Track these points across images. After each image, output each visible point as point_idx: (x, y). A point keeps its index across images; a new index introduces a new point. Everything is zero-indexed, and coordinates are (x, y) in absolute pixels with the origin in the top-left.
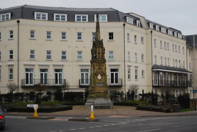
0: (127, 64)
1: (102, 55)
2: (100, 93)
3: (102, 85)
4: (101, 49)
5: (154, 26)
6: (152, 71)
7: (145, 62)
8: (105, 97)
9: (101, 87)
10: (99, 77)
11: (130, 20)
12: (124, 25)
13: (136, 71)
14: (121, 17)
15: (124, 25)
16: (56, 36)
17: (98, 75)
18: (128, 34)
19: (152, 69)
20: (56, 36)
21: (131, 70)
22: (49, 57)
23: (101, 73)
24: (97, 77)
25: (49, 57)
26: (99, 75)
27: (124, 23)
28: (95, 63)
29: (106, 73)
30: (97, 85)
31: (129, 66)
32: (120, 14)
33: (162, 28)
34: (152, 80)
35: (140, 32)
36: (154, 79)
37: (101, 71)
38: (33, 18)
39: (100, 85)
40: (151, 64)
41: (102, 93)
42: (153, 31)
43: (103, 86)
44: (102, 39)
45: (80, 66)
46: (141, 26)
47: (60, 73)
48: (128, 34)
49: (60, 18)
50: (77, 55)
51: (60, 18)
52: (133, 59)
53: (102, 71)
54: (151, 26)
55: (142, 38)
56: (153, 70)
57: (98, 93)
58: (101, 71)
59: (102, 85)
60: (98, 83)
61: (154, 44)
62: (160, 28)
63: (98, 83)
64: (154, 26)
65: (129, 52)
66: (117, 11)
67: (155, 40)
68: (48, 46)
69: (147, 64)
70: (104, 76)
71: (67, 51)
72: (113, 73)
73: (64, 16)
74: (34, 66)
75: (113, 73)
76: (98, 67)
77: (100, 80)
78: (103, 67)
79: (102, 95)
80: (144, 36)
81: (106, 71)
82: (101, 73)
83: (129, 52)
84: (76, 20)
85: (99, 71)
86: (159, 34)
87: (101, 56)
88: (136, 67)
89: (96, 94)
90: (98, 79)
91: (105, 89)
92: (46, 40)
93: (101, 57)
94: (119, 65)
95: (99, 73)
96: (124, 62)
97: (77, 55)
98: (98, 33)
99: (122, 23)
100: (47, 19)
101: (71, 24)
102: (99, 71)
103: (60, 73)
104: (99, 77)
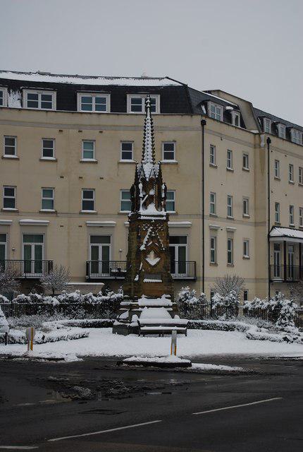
0: (208, 222)
5: (274, 126)
7: (252, 220)
11: (215, 111)
12: (203, 123)
13: (230, 243)
14: (195, 103)
15: (203, 123)
18: (212, 148)
20: (29, 148)
21: (218, 238)
27: (204, 118)
31: (214, 230)
32: (191, 95)
33: (292, 131)
34: (269, 265)
35: (235, 142)
36: (272, 263)
40: (267, 224)
42: (272, 138)
45: (90, 226)
46: (243, 125)
48: (212, 148)
49: (40, 101)
51: (40, 101)
52: (222, 209)
54: (267, 127)
55: (245, 158)
61: (275, 173)
62: (288, 130)
64: (274, 126)
66: (185, 86)
67: (277, 162)
69: (256, 224)
72: (174, 247)
73: (50, 98)
75: (174, 247)
80: (250, 151)
84: (79, 109)
86: (286, 145)
88: (230, 232)
94: (187, 227)
96: (201, 220)
99: (197, 120)
100: (108, 110)
101: (65, 118)
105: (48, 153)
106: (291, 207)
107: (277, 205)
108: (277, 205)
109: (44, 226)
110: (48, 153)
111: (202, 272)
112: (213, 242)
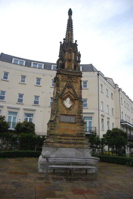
0: (101, 113)
1: (75, 67)
2: (68, 136)
3: (73, 120)
4: (73, 54)
6: (121, 124)
8: (77, 146)
10: (68, 103)
13: (108, 122)
16: (31, 81)
17: (65, 99)
19: (121, 123)
20: (31, 81)
22: (20, 101)
23: (73, 97)
24: (62, 102)
25: (20, 101)
26: (68, 99)
29: (81, 96)
30: (63, 118)
31: (103, 116)
37: (71, 91)
38: (11, 62)
39: (67, 119)
41: (72, 136)
43: (74, 121)
44: (76, 41)
47: (30, 118)
50: (51, 101)
53: (74, 91)
56: (122, 124)
57: (63, 135)
59: (73, 120)
60: (63, 115)
63: (63, 115)
68: (22, 89)
69: (116, 118)
70: (77, 102)
71: (40, 97)
74: (2, 108)
76: (65, 84)
77: (69, 109)
79: (71, 141)
81: (81, 92)
82: (73, 97)
85: (67, 90)
87: (73, 65)
88: (108, 118)
89: (58, 137)
90: (64, 106)
91: (78, 128)
92: (19, 83)
93: (73, 68)
95: (68, 96)
96: (98, 111)
97: (51, 101)
98: (70, 32)
102: (67, 90)
103: (30, 118)
104: (68, 103)
105: (38, 83)
106: (126, 115)
107: (122, 112)
108: (122, 112)
109: (34, 110)
110: (38, 83)
111: (98, 133)
112: (102, 120)
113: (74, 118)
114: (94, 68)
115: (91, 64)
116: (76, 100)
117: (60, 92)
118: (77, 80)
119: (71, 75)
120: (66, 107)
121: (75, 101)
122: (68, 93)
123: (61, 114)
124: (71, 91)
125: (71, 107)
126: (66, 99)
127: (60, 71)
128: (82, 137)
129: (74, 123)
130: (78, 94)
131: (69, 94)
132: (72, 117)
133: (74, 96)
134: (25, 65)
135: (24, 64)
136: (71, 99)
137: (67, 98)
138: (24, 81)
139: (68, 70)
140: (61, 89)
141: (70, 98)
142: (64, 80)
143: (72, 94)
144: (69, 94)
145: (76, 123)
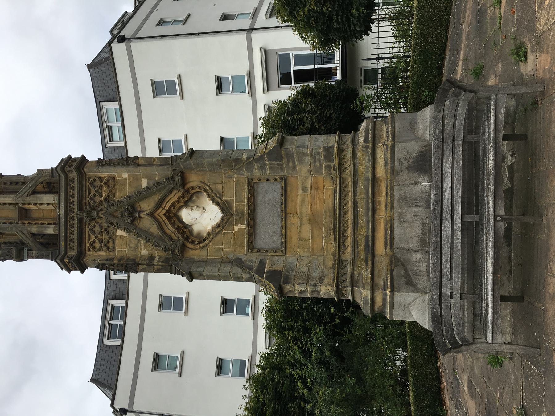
9: (285, 204)
23: (172, 199)
28: (91, 256)
53: (148, 192)
58: (146, 206)
65: (225, 17)
70: (194, 180)
72: (294, 71)
75: (294, 71)
76: (120, 233)
78: (123, 182)
82: (172, 199)
83: (225, 17)
89: (348, 255)
91: (303, 169)
94: (266, 53)
102: (147, 223)
113: (262, 188)
114: (101, 58)
115: (89, 67)
116: (184, 183)
117: (159, 253)
118: (101, 179)
119: (81, 208)
120: (218, 226)
121: (191, 184)
122: (155, 219)
123: (251, 246)
124: (146, 206)
125: (218, 204)
126: (186, 226)
127: (70, 258)
128: (340, 150)
129: (285, 193)
130: (159, 174)
131: (161, 213)
132: (260, 198)
133: (171, 192)
134: (124, 302)
135: (120, 303)
136: (186, 204)
137: (181, 221)
138: (178, 300)
139: (62, 220)
140: (144, 252)
141: (180, 209)
142: (105, 237)
143: (166, 196)
144: (161, 213)
145: (285, 179)
